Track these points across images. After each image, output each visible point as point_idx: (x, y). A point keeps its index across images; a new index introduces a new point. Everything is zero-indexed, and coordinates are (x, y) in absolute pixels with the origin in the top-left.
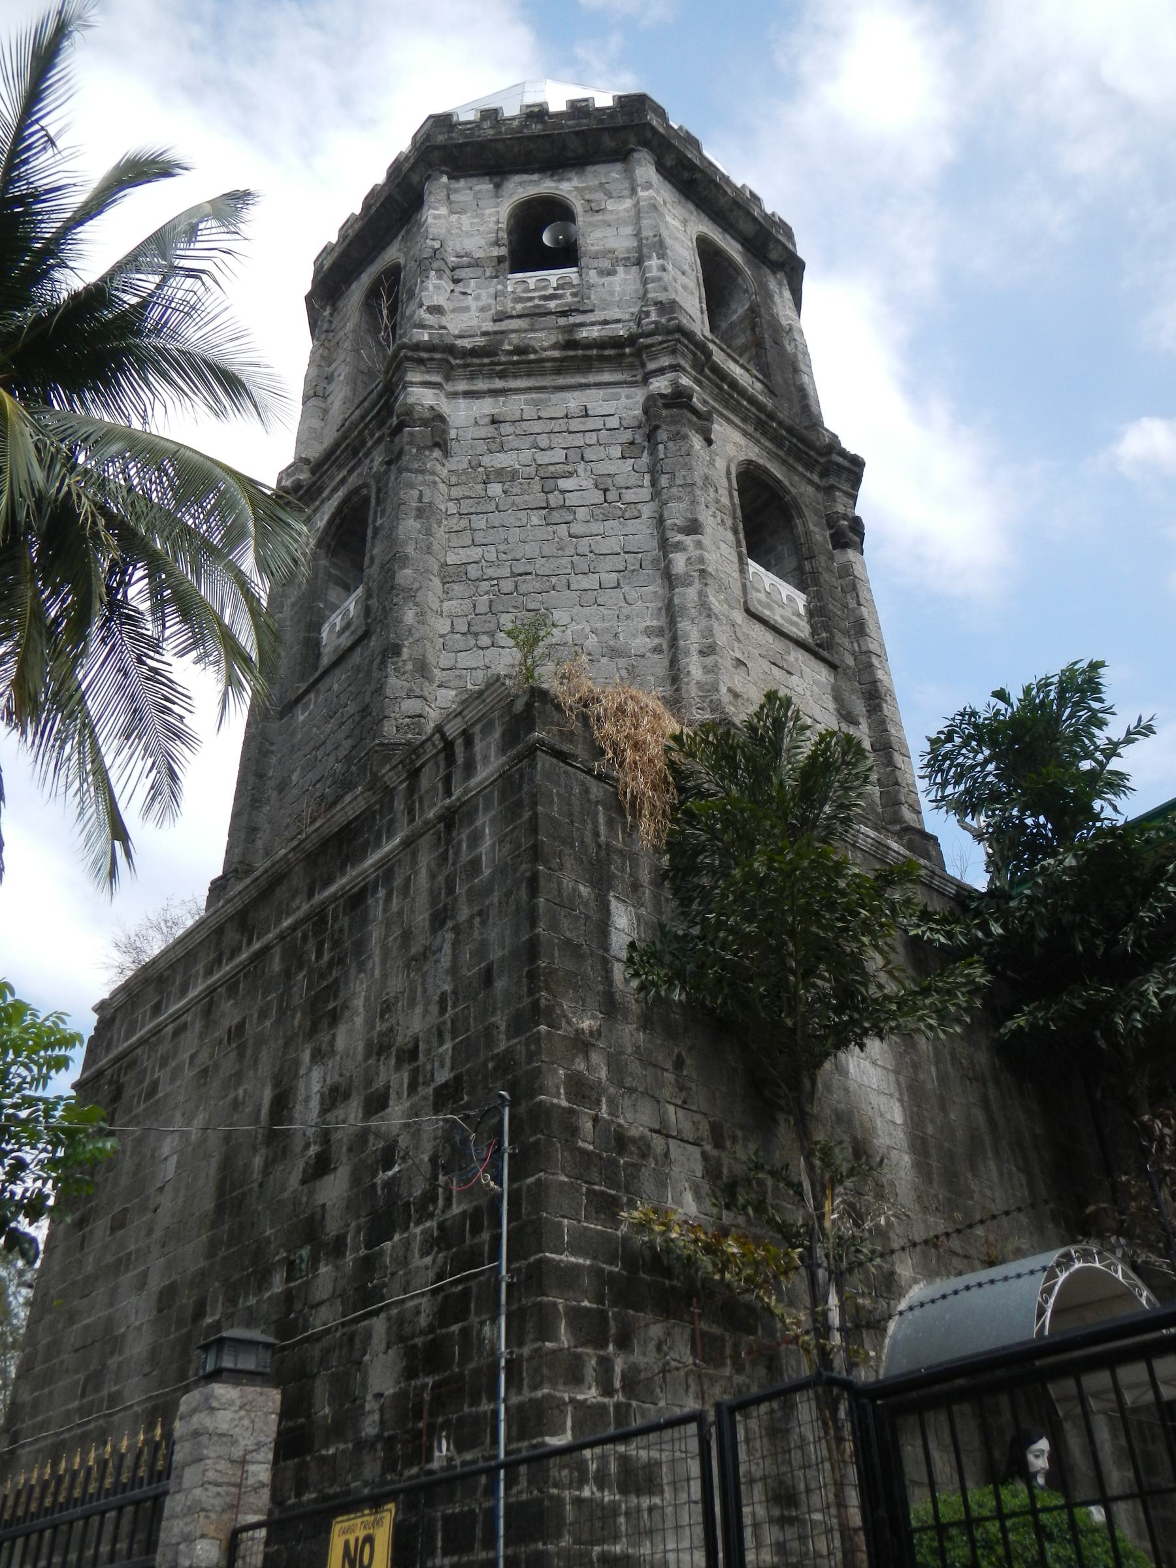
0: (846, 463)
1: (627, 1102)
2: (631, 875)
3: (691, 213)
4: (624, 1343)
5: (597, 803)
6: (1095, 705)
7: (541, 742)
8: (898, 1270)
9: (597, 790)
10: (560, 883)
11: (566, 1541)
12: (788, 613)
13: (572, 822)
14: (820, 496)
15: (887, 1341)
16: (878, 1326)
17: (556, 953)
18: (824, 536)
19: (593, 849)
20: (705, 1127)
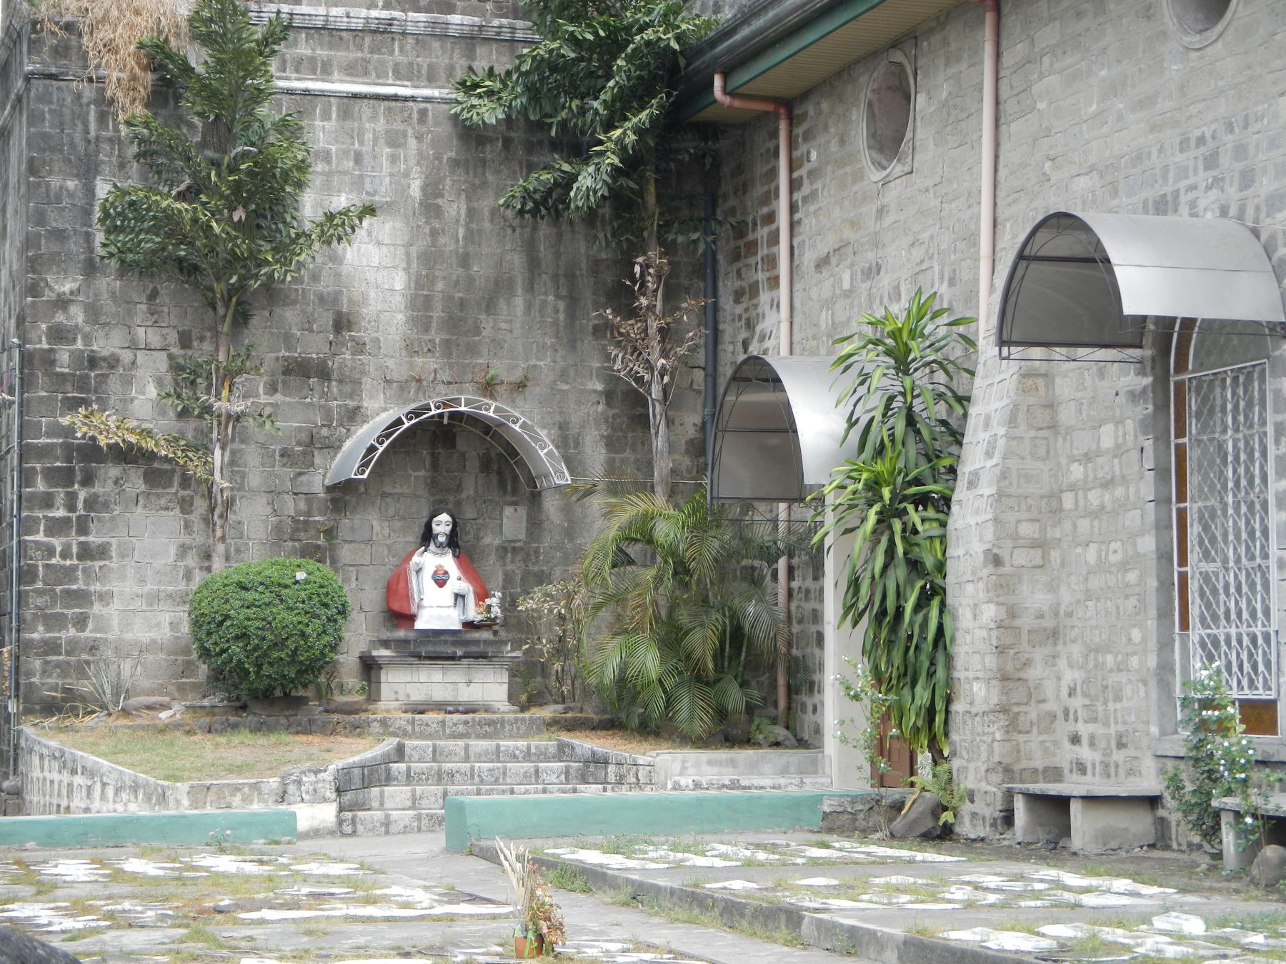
1: (101, 333)
2: (119, 156)
4: (87, 481)
5: (88, 105)
7: (32, 73)
8: (365, 404)
9: (88, 92)
10: (48, 185)
11: (39, 585)
13: (62, 131)
15: (339, 455)
16: (332, 446)
17: (43, 242)
19: (81, 147)
20: (173, 336)
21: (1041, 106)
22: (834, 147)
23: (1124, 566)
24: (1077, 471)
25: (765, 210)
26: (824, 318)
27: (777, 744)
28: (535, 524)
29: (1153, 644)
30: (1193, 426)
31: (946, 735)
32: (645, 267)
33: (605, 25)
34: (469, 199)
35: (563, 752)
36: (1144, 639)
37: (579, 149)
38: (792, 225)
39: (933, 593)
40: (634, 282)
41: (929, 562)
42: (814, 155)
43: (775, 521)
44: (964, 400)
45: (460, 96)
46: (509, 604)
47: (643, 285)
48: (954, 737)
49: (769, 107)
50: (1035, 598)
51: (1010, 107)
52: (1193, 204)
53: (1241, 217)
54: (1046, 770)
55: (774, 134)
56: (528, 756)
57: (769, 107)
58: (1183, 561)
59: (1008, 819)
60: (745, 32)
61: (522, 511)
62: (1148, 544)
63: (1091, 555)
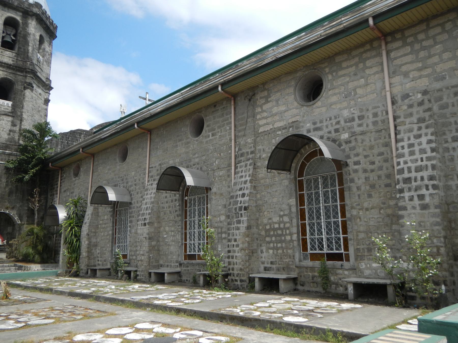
0: (30, 71)
3: (5, 11)
6: (49, 127)
12: (6, 107)
14: (24, 78)
18: (22, 88)
21: (99, 171)
22: (68, 175)
23: (107, 236)
24: (101, 222)
25: (56, 183)
26: (64, 199)
27: (52, 263)
28: (14, 229)
29: (110, 247)
30: (118, 216)
31: (79, 260)
32: (36, 191)
33: (32, 155)
34: (7, 179)
35: (15, 266)
36: (109, 246)
37: (26, 172)
38: (61, 186)
39: (79, 240)
40: (34, 193)
41: (78, 235)
42: (65, 176)
43: (54, 229)
44: (85, 212)
45: (7, 163)
46: (7, 242)
47: (35, 193)
48: (80, 261)
49: (58, 168)
50: (94, 240)
51: (95, 171)
52: (120, 186)
53: (126, 188)
54: (94, 265)
55: (59, 172)
56: (8, 266)
57: (58, 168)
58: (115, 235)
59: (87, 273)
60: (55, 157)
61: (11, 228)
62: (111, 232)
63: (102, 234)
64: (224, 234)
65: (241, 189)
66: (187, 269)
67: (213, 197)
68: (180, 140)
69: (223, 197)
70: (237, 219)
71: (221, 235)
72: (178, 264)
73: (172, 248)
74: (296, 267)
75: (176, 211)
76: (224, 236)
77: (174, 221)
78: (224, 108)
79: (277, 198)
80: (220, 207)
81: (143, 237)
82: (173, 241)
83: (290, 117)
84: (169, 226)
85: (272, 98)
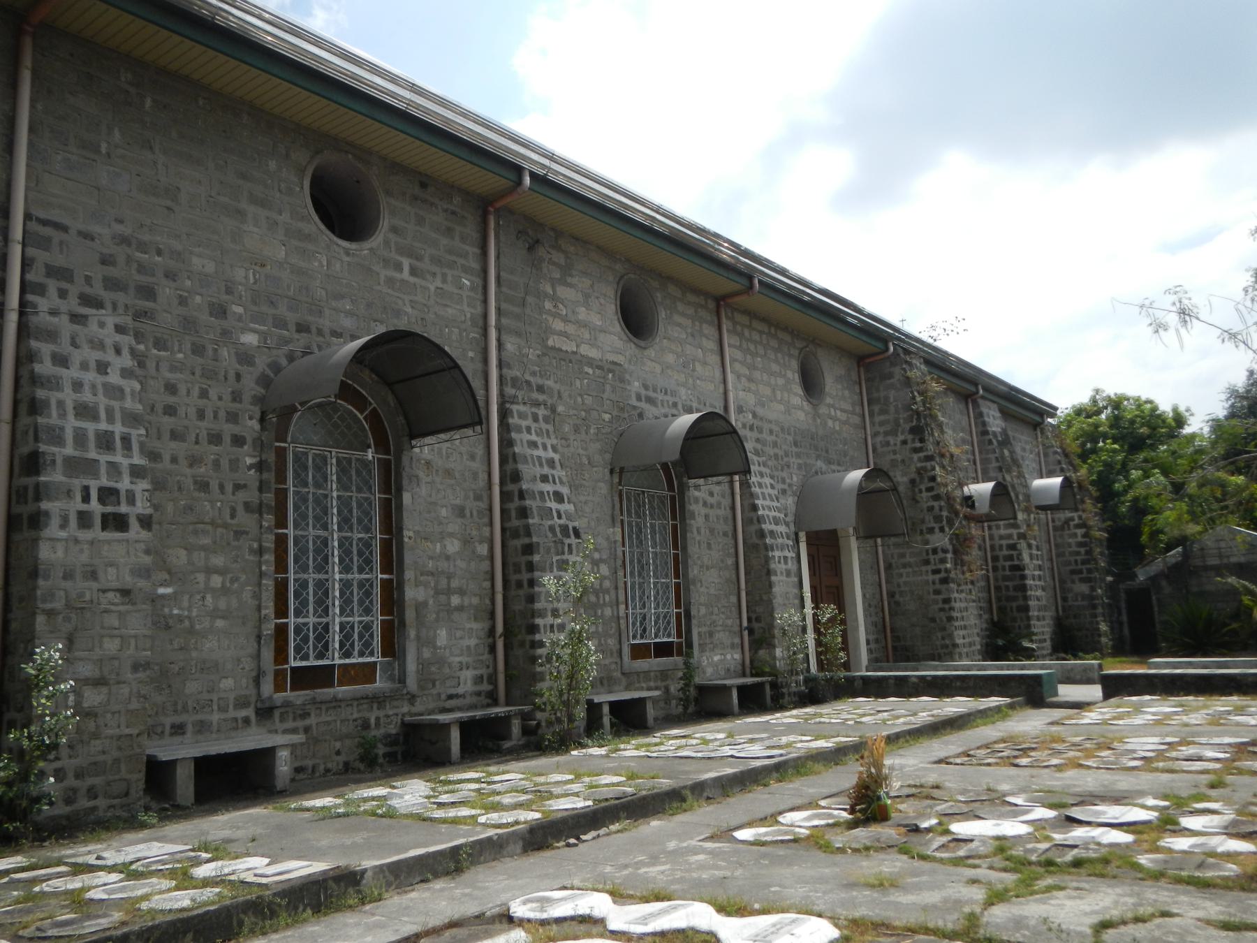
64: (456, 596)
65: (544, 479)
66: (300, 724)
67: (421, 474)
68: (263, 203)
69: (453, 482)
70: (559, 557)
71: (449, 598)
72: (249, 712)
73: (210, 644)
74: (623, 674)
75: (238, 487)
76: (455, 600)
77: (225, 526)
78: (453, 213)
79: (586, 520)
80: (444, 512)
81: (95, 585)
82: (215, 614)
83: (609, 349)
84: (189, 549)
85: (575, 280)
